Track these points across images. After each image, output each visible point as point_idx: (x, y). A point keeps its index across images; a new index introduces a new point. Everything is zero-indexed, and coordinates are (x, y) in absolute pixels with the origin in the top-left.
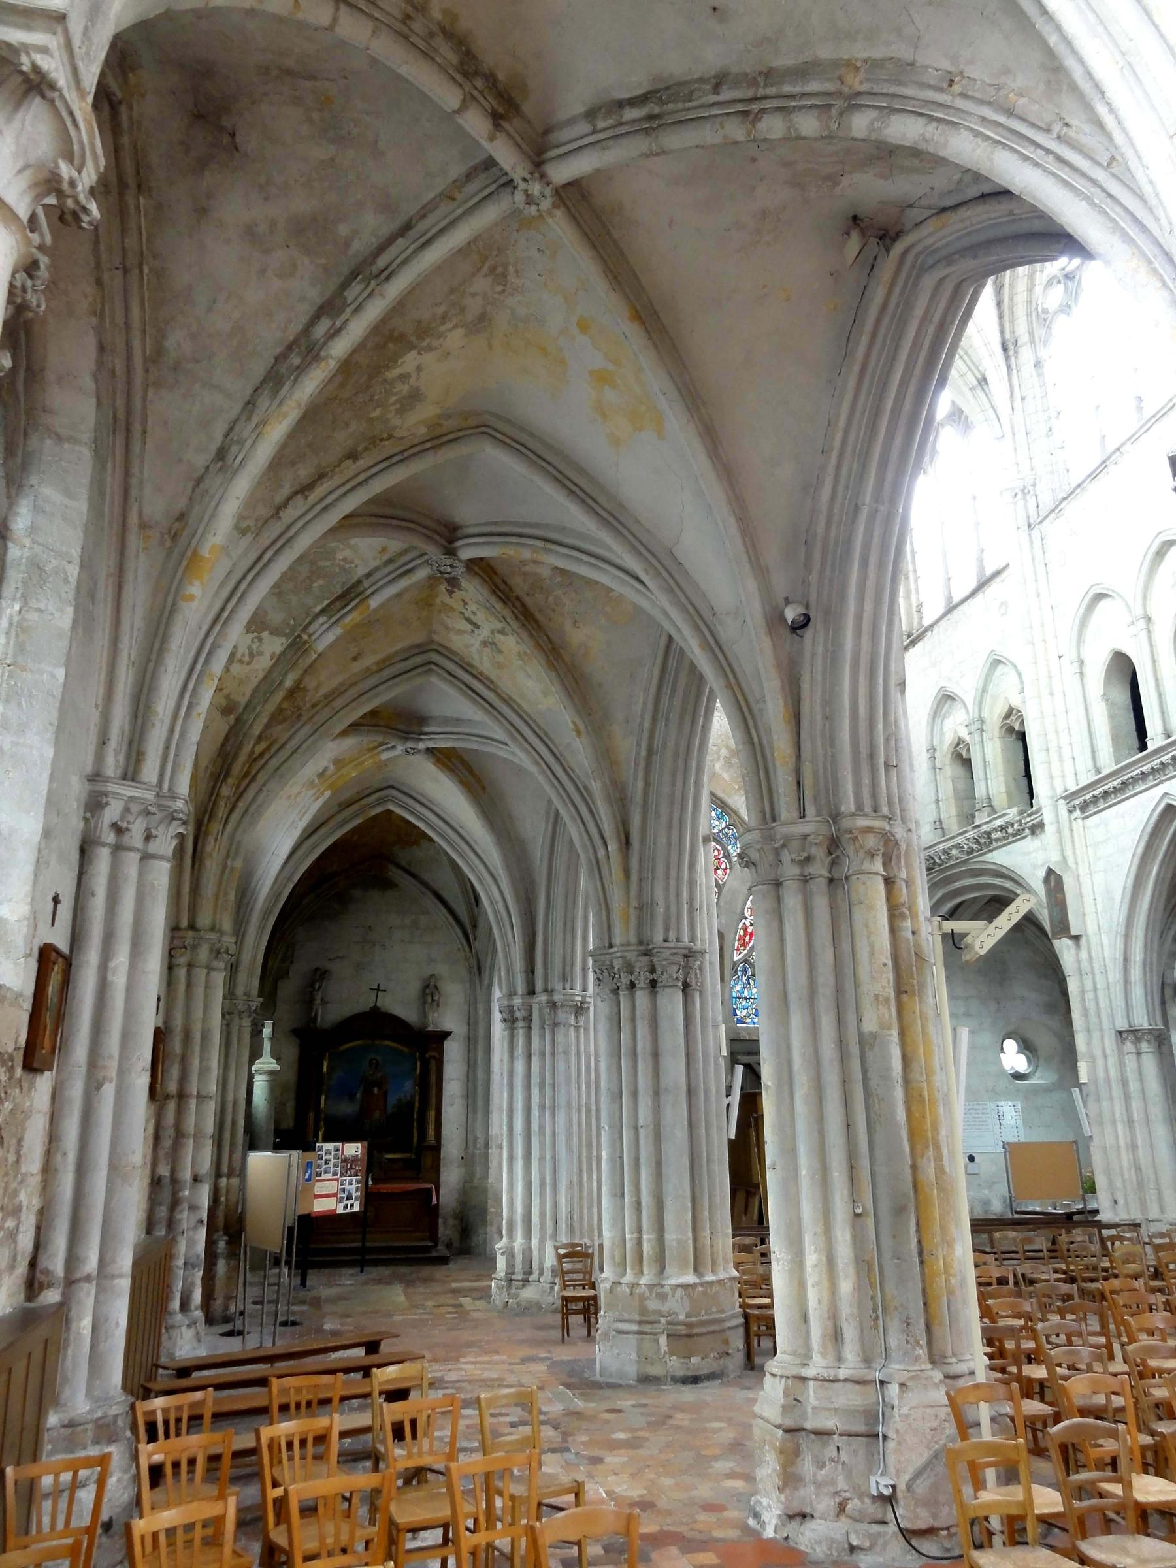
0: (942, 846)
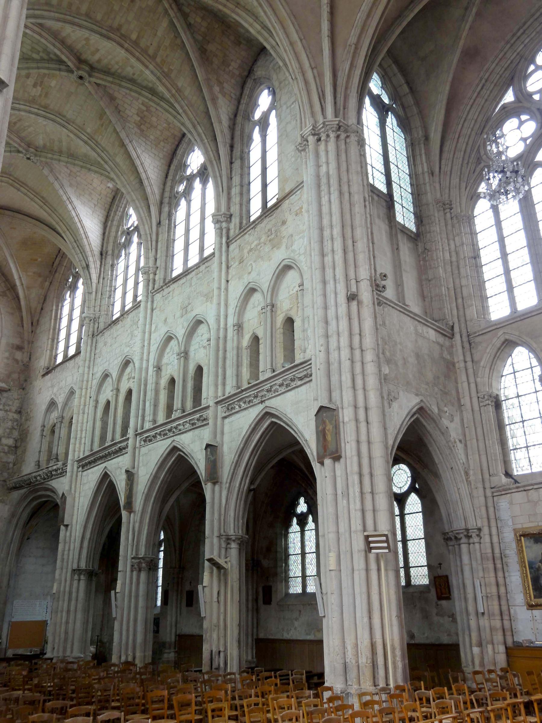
0: (34, 474)
